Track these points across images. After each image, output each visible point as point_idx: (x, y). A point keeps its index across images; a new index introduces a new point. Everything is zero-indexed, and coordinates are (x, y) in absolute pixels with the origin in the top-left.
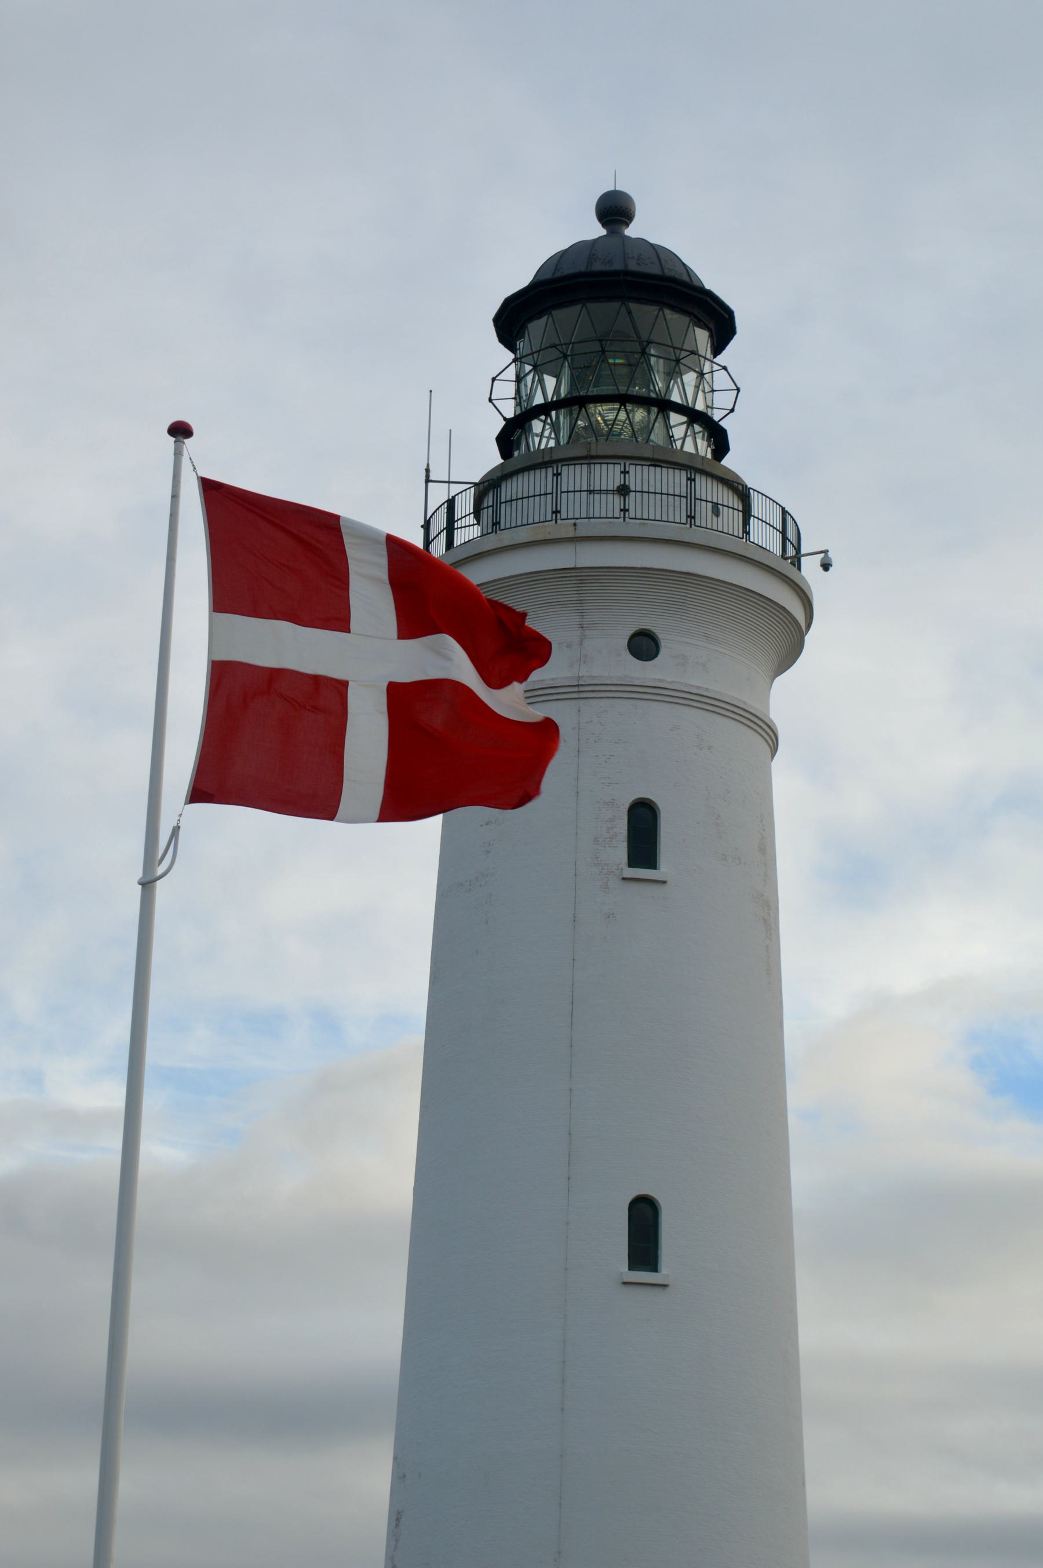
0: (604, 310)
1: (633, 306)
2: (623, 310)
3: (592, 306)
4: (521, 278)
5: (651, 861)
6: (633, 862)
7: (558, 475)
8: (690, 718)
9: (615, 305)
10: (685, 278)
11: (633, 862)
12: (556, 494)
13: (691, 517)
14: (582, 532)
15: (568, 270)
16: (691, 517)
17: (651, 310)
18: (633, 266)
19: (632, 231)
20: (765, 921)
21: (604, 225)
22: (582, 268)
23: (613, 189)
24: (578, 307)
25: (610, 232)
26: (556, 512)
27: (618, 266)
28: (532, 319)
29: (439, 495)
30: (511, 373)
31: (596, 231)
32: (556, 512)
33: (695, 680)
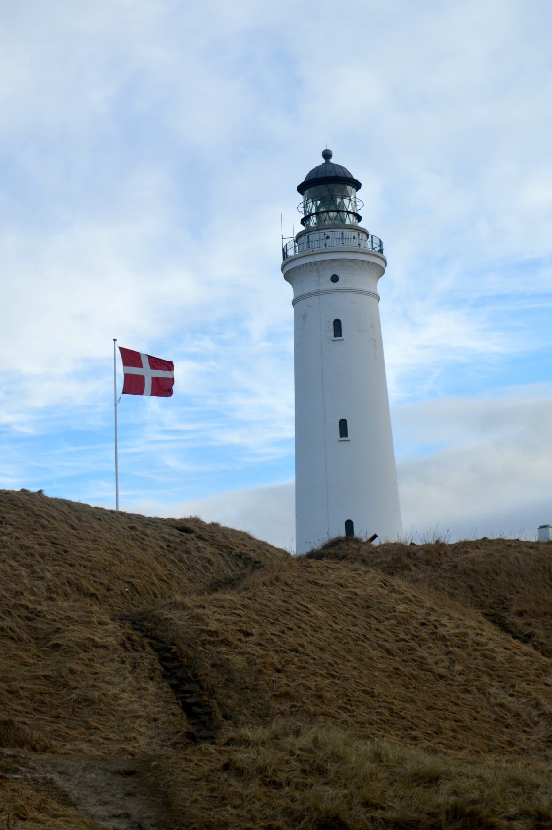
0: (321, 187)
1: (328, 185)
2: (326, 188)
3: (318, 187)
4: (302, 180)
5: (341, 336)
6: (335, 336)
7: (308, 237)
8: (348, 296)
9: (323, 186)
10: (343, 175)
11: (335, 336)
12: (309, 242)
13: (343, 244)
14: (314, 252)
15: (312, 178)
16: (343, 244)
17: (334, 185)
18: (328, 175)
19: (332, 160)
20: (374, 345)
21: (325, 159)
22: (314, 177)
23: (325, 149)
24: (314, 188)
25: (326, 161)
26: (309, 247)
27: (323, 175)
28: (305, 190)
29: (285, 242)
30: (302, 205)
31: (323, 161)
32: (309, 247)
33: (349, 286)
